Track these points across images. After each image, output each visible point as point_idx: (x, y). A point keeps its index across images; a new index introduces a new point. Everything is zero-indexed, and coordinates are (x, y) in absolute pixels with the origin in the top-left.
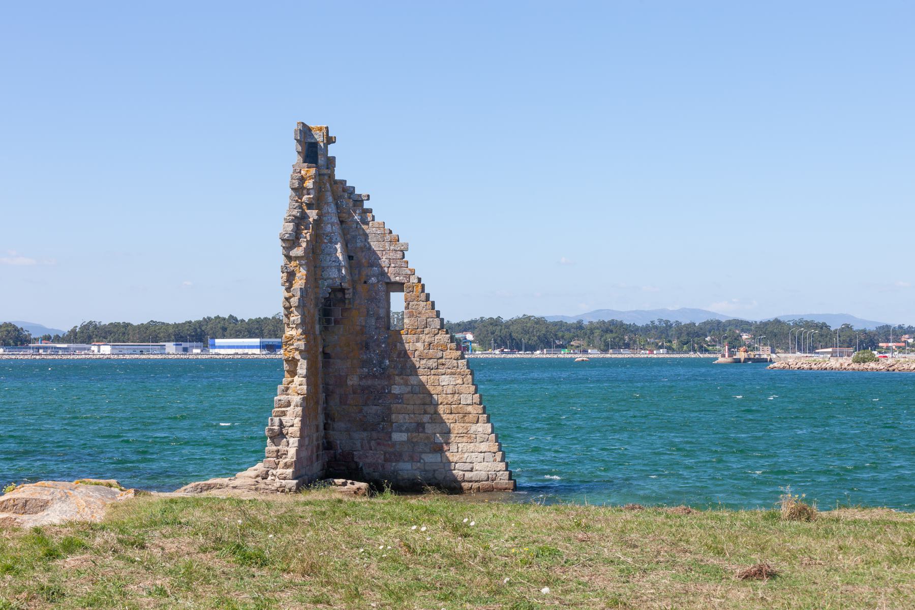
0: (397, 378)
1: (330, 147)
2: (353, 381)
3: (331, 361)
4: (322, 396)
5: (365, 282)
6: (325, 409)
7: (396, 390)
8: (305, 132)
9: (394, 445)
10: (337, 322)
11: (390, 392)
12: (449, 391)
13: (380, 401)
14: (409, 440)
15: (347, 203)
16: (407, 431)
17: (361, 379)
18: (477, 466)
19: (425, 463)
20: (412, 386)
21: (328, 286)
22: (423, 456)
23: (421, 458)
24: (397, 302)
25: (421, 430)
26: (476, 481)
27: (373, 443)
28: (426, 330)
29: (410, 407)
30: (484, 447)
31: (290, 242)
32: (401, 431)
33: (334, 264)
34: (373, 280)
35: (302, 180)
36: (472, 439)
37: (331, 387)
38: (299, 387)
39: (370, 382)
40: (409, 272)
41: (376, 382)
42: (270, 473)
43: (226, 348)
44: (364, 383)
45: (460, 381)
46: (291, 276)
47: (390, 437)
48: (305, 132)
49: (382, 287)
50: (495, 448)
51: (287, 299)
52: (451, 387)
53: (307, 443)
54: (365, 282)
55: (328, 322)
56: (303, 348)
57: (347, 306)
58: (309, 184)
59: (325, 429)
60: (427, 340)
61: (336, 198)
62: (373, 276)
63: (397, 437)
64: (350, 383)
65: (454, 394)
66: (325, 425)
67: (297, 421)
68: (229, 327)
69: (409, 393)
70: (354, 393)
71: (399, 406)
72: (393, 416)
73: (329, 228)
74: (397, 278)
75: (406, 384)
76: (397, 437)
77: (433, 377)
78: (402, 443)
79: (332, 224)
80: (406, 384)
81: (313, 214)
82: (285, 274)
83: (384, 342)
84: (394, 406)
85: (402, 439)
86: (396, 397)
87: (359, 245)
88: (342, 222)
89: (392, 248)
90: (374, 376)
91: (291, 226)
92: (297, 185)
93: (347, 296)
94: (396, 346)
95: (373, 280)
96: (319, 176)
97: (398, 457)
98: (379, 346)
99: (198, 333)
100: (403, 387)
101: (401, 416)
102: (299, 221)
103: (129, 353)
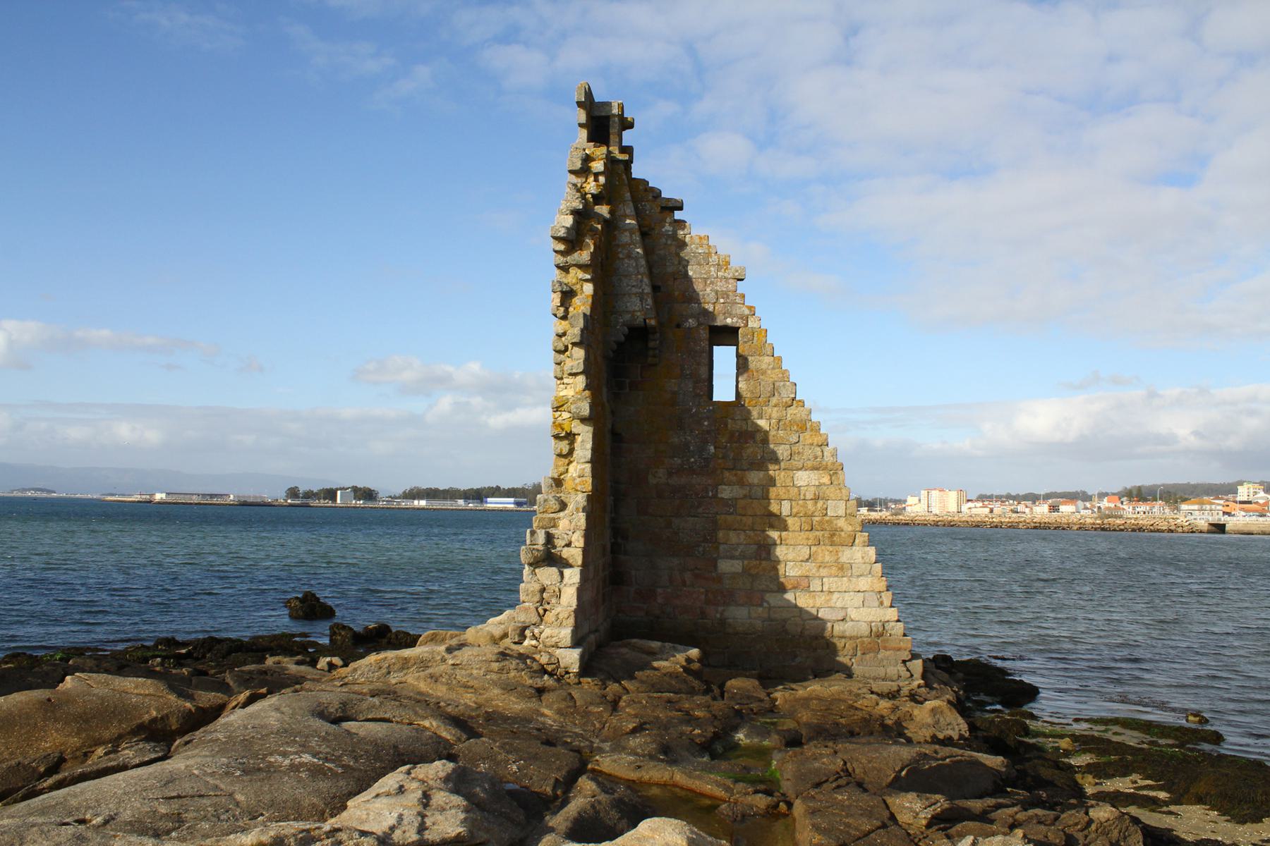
0: (727, 474)
1: (626, 134)
2: (659, 477)
4: (610, 500)
6: (613, 520)
7: (726, 492)
8: (588, 103)
9: (719, 579)
11: (715, 496)
13: (700, 510)
14: (746, 571)
15: (651, 209)
16: (743, 557)
17: (670, 474)
18: (853, 614)
19: (770, 608)
20: (751, 486)
21: (624, 324)
22: (768, 596)
23: (763, 600)
24: (724, 357)
25: (764, 555)
26: (851, 638)
27: (688, 576)
28: (774, 400)
29: (749, 520)
30: (864, 583)
31: (571, 241)
32: (732, 558)
33: (634, 290)
34: (691, 322)
35: (587, 159)
36: (843, 569)
38: (578, 480)
40: (747, 312)
42: (528, 632)
43: (493, 503)
44: (675, 481)
45: (826, 480)
46: (567, 295)
47: (715, 567)
48: (588, 103)
49: (704, 334)
50: (882, 585)
51: (560, 336)
53: (591, 576)
54: (678, 326)
56: (586, 411)
57: (650, 360)
58: (598, 166)
59: (613, 552)
60: (775, 415)
61: (635, 200)
62: (692, 316)
63: (726, 566)
65: (816, 499)
66: (613, 545)
67: (578, 540)
68: (496, 492)
69: (745, 497)
71: (730, 518)
72: (721, 534)
73: (625, 238)
74: (729, 321)
75: (741, 483)
76: (726, 566)
78: (734, 576)
79: (631, 231)
80: (741, 483)
81: (603, 210)
82: (559, 295)
83: (708, 418)
84: (721, 518)
85: (733, 570)
86: (725, 502)
87: (670, 270)
91: (569, 221)
92: (578, 165)
93: (651, 344)
95: (691, 322)
96: (610, 161)
97: (729, 598)
99: (478, 495)
101: (732, 534)
102: (582, 216)
103: (437, 504)
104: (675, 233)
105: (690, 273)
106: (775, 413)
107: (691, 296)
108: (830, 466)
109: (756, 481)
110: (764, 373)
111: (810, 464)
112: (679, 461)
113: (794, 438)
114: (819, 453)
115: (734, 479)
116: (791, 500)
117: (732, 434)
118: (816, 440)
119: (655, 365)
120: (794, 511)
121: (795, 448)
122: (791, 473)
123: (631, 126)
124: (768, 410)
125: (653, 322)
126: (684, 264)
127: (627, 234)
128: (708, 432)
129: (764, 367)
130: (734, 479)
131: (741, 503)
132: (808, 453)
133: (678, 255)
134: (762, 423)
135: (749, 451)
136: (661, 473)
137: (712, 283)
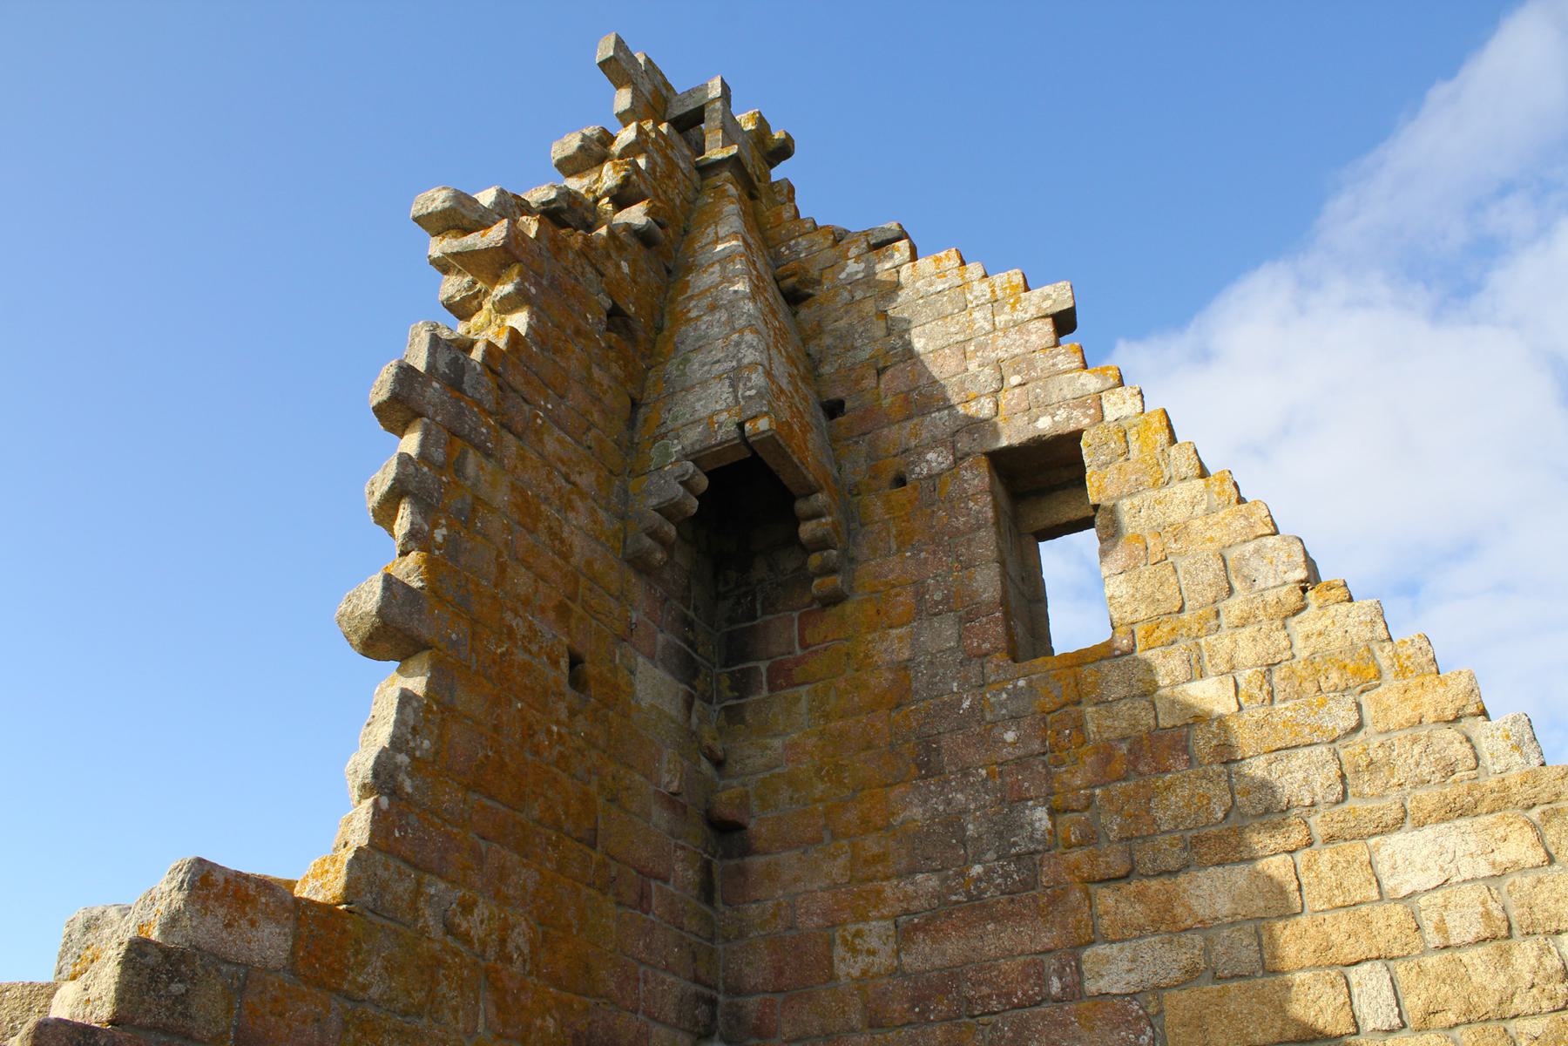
0: (1106, 898)
2: (866, 953)
3: (757, 862)
5: (900, 481)
7: (1112, 970)
10: (782, 677)
11: (1074, 992)
12: (1464, 926)
17: (904, 935)
28: (1234, 608)
37: (752, 1003)
39: (953, 948)
41: (995, 940)
44: (924, 956)
45: (1519, 847)
52: (1471, 896)
54: (900, 481)
55: (743, 685)
62: (935, 443)
64: (848, 967)
69: (1192, 976)
70: (875, 1022)
75: (1167, 923)
77: (1326, 856)
80: (1167, 923)
83: (1015, 718)
87: (865, 354)
88: (795, 297)
89: (1001, 319)
90: (977, 909)
94: (1079, 726)
95: (936, 459)
98: (988, 740)
100: (1151, 947)
104: (870, 273)
105: (919, 344)
106: (1248, 648)
107: (925, 397)
108: (1520, 793)
109: (1224, 907)
110: (1180, 531)
111: (1428, 797)
112: (928, 882)
113: (1344, 716)
114: (1460, 750)
115: (1136, 913)
116: (1386, 958)
117: (1106, 754)
118: (1435, 700)
119: (834, 599)
120: (1414, 1004)
121: (1352, 751)
122: (1359, 849)
123: (784, 150)
124: (1220, 643)
125: (763, 424)
126: (898, 329)
127: (717, 267)
128: (1021, 763)
129: (1177, 515)
130: (1136, 913)
131: (1179, 1004)
132: (1408, 758)
133: (883, 314)
134: (1210, 694)
135: (1176, 799)
136: (876, 932)
137: (981, 347)
